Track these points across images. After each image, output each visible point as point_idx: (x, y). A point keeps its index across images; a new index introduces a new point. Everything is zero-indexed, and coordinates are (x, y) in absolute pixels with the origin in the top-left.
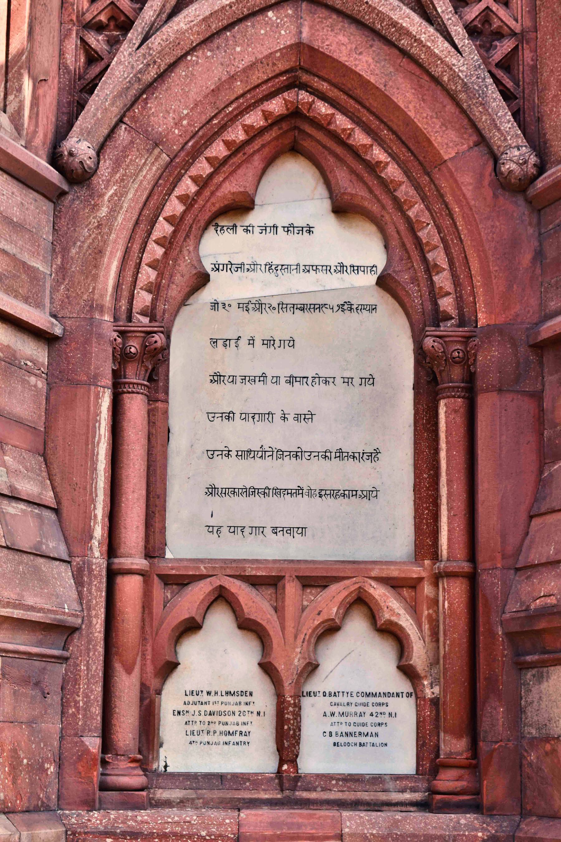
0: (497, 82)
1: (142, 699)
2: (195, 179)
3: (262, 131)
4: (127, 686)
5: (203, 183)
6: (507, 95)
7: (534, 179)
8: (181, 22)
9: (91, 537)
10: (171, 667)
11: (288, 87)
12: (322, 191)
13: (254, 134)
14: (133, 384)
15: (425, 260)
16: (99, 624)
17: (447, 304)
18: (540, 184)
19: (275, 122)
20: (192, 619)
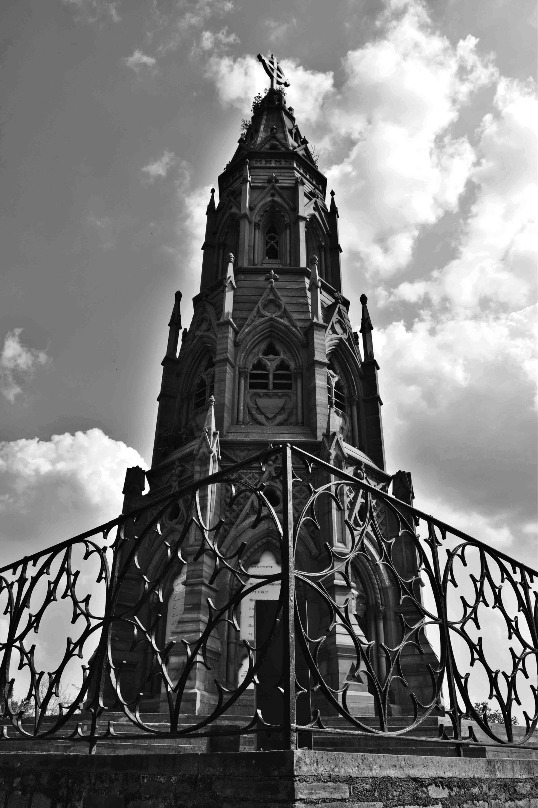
0: (310, 535)
1: (235, 671)
2: (247, 556)
3: (261, 546)
4: (232, 668)
5: (248, 557)
6: (312, 539)
7: (318, 557)
8: (244, 524)
9: (224, 634)
10: (241, 665)
11: (267, 537)
12: (274, 558)
13: (259, 547)
16: (226, 654)
18: (319, 558)
19: (264, 544)
20: (245, 654)
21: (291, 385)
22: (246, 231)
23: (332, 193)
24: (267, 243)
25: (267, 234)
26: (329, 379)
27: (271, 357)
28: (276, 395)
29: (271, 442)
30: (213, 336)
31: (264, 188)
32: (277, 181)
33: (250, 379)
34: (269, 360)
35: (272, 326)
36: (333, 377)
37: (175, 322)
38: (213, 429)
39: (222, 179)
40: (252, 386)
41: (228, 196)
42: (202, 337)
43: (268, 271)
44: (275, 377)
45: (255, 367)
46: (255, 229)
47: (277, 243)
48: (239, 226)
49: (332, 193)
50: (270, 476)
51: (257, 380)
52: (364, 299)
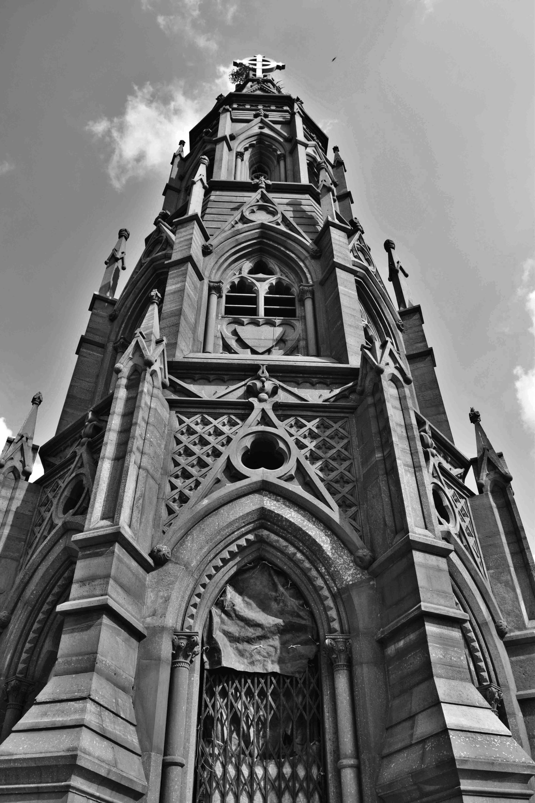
14: (182, 662)
15: (323, 604)
17: (336, 625)
18: (375, 565)
21: (294, 310)
23: (336, 149)
25: (253, 174)
27: (261, 276)
29: (263, 365)
33: (227, 303)
35: (262, 235)
38: (157, 334)
39: (193, 134)
42: (152, 261)
44: (267, 301)
46: (236, 158)
49: (336, 149)
50: (262, 418)
52: (389, 246)
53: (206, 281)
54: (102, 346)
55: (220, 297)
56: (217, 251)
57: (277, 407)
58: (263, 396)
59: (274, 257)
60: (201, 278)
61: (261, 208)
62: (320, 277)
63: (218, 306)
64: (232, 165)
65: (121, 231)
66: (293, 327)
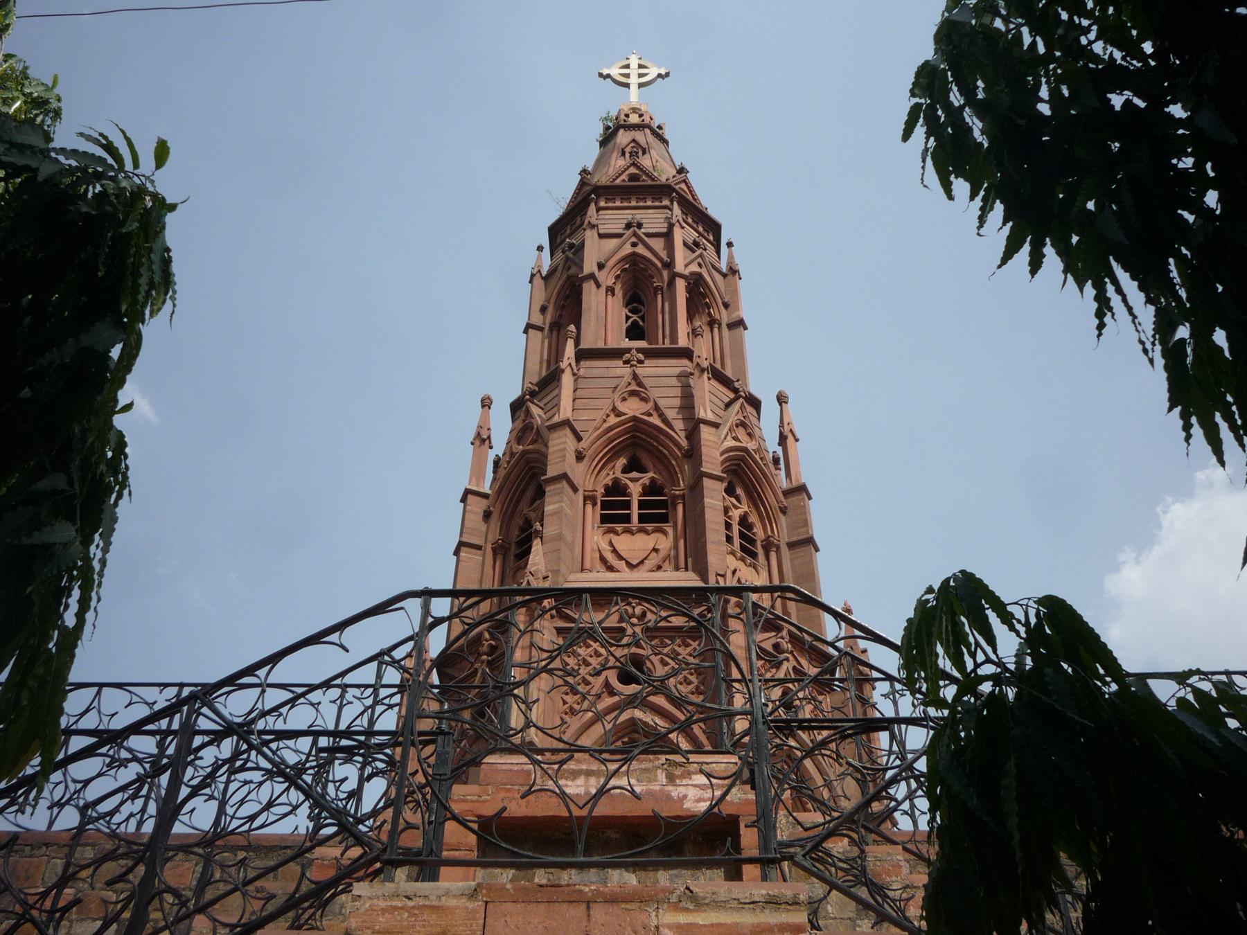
22: (592, 298)
23: (730, 245)
24: (628, 318)
26: (726, 510)
27: (635, 474)
28: (642, 530)
30: (543, 449)
31: (619, 236)
32: (640, 226)
34: (632, 480)
36: (736, 508)
37: (482, 440)
40: (605, 519)
41: (563, 252)
42: (524, 453)
43: (628, 350)
44: (642, 505)
45: (609, 491)
47: (642, 318)
48: (581, 293)
49: (730, 245)
51: (613, 510)
52: (781, 399)
53: (581, 492)
54: (479, 548)
55: (594, 504)
56: (589, 454)
57: (647, 630)
58: (634, 620)
59: (646, 449)
60: (575, 490)
61: (633, 393)
62: (692, 482)
63: (593, 514)
64: (604, 316)
65: (482, 401)
66: (665, 533)
